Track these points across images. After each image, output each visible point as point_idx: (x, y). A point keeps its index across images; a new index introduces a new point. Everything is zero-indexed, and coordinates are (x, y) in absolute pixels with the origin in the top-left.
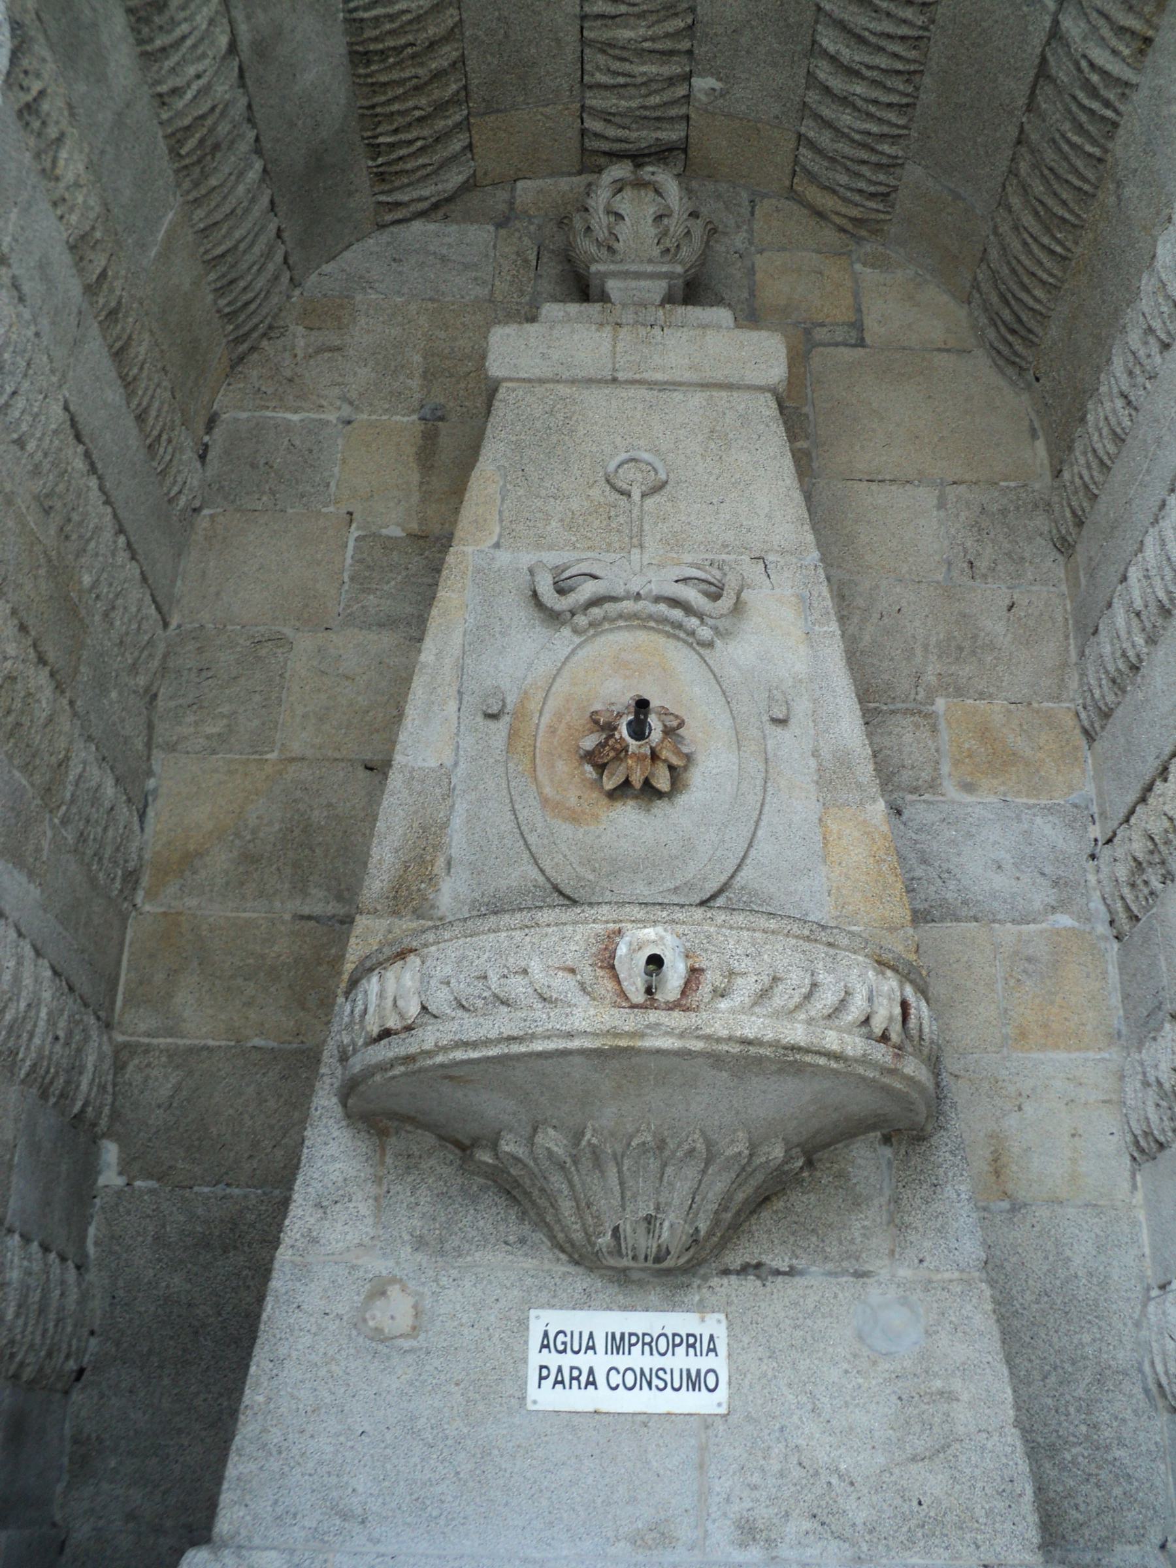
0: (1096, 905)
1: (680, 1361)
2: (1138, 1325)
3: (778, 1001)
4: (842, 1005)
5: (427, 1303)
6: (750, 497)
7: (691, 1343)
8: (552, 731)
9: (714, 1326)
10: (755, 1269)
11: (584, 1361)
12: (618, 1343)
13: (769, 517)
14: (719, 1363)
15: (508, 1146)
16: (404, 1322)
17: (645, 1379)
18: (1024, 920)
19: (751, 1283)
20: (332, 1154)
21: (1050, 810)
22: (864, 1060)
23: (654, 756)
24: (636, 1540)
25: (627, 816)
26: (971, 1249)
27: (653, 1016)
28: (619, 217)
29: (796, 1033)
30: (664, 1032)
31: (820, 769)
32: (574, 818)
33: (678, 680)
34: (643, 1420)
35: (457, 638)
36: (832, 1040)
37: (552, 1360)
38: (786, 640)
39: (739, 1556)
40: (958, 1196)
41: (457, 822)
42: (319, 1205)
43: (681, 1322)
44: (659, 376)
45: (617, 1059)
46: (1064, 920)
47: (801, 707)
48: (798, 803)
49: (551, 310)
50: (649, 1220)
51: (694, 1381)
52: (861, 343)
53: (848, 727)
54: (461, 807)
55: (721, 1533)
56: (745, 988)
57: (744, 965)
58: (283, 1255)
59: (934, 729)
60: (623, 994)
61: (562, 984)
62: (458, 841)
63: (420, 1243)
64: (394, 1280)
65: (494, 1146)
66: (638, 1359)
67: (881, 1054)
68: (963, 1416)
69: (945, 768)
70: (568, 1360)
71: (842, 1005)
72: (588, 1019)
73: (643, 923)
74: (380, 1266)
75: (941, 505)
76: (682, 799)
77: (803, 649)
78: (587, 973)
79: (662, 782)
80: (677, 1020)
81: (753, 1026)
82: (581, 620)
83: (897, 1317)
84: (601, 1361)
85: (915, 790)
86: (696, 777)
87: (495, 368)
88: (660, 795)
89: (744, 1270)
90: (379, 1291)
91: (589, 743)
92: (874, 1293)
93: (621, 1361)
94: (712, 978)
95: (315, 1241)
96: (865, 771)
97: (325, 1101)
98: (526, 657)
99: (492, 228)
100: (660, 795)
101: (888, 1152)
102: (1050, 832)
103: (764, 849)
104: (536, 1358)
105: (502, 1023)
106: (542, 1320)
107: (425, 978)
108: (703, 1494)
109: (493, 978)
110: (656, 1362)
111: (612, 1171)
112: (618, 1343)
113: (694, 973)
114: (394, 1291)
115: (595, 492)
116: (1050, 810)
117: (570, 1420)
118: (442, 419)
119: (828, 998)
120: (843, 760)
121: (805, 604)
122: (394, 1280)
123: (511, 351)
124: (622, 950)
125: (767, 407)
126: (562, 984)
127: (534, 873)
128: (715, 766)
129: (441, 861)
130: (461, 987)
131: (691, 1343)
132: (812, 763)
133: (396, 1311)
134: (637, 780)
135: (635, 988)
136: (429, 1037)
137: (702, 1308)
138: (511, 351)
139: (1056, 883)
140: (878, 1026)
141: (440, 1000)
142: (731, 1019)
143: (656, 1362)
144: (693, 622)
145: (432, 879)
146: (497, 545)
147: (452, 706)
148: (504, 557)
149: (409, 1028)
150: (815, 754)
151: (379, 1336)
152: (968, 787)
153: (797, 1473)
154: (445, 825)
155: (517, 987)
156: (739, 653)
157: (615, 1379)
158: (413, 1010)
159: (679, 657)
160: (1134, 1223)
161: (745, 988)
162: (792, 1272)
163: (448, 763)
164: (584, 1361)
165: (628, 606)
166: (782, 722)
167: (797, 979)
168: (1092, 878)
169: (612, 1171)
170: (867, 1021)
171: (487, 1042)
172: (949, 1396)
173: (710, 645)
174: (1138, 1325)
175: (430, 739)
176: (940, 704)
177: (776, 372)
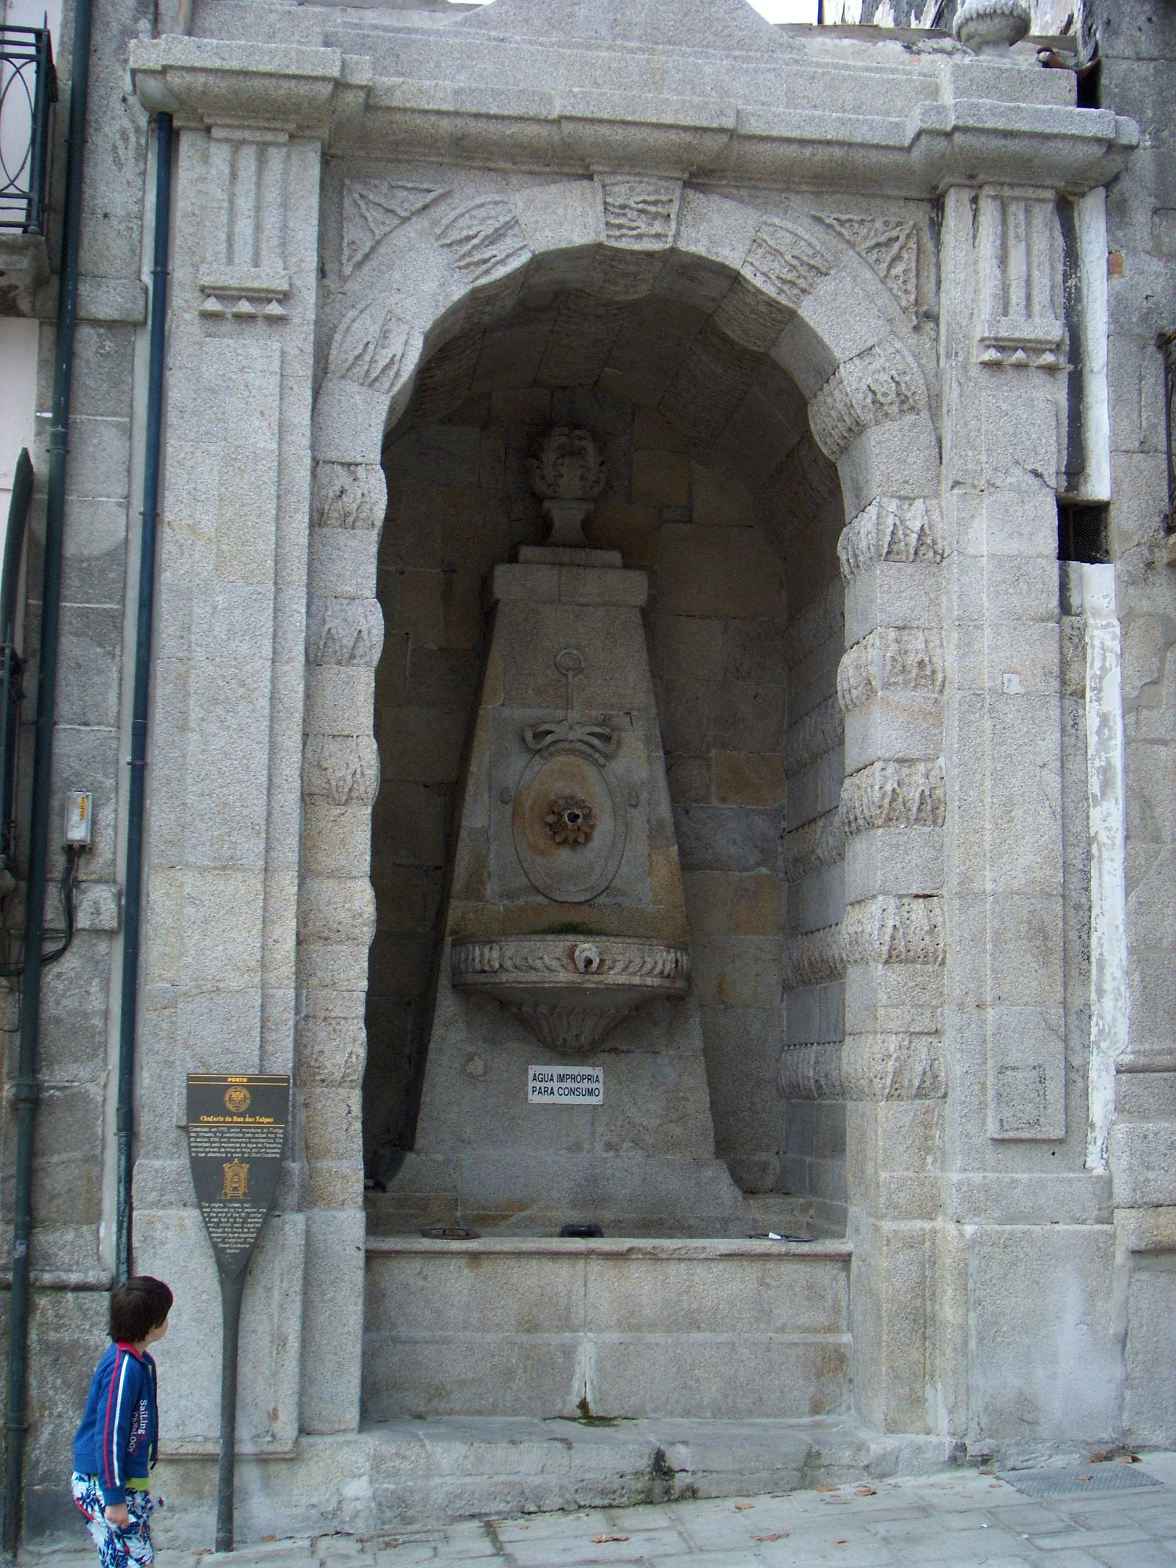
0: (780, 863)
1: (585, 1085)
2: (777, 1061)
3: (631, 970)
4: (653, 968)
5: (489, 1063)
6: (625, 680)
7: (590, 1078)
8: (532, 808)
9: (598, 1072)
10: (615, 1050)
11: (549, 1085)
12: (562, 1078)
13: (634, 688)
14: (600, 1086)
15: (525, 1009)
16: (481, 1070)
17: (572, 1092)
18: (745, 869)
19: (613, 1056)
20: (447, 1005)
21: (763, 813)
22: (660, 986)
23: (579, 829)
24: (569, 1149)
25: (565, 854)
26: (698, 1043)
27: (587, 977)
28: (561, 476)
29: (637, 980)
30: (592, 982)
31: (651, 829)
32: (543, 854)
33: (591, 787)
34: (572, 1107)
35: (486, 758)
36: (649, 981)
37: (538, 1084)
38: (638, 760)
39: (605, 1155)
40: (695, 1023)
41: (492, 856)
42: (444, 1025)
43: (586, 1070)
44: (582, 600)
45: (574, 990)
46: (764, 870)
47: (644, 796)
48: (640, 847)
49: (526, 552)
50: (577, 1036)
51: (590, 1092)
52: (690, 521)
53: (664, 809)
54: (493, 848)
55: (599, 1147)
56: (619, 966)
57: (619, 957)
58: (432, 1045)
59: (709, 768)
60: (577, 968)
61: (554, 964)
62: (493, 866)
63: (485, 1040)
64: (475, 1054)
65: (520, 1006)
66: (570, 1084)
67: (667, 983)
68: (690, 1107)
69: (713, 789)
70: (543, 1084)
71: (653, 968)
72: (564, 977)
73: (585, 942)
74: (471, 1049)
75: (725, 633)
76: (590, 845)
77: (646, 765)
78: (565, 961)
79: (582, 840)
80: (596, 978)
81: (622, 979)
82: (545, 754)
83: (668, 1069)
84: (555, 1085)
85: (697, 801)
86: (596, 834)
87: (500, 591)
88: (579, 843)
89: (610, 1051)
90: (470, 1058)
91: (550, 819)
92: (659, 1060)
93: (563, 1085)
94: (608, 963)
95: (444, 1039)
96: (670, 830)
97: (444, 982)
98: (518, 770)
99: (478, 429)
100: (579, 843)
101: (668, 1004)
102: (762, 824)
103: (624, 869)
104: (531, 1084)
105: (532, 977)
106: (534, 1070)
107: (502, 957)
108: (593, 1134)
109: (530, 961)
110: (576, 1085)
111: (565, 1018)
112: (562, 1078)
113: (602, 961)
114: (476, 1058)
115: (549, 672)
116: (763, 813)
117: (544, 1107)
118: (453, 571)
119: (649, 966)
120: (661, 824)
121: (648, 740)
122: (475, 1054)
123: (509, 582)
124: (577, 953)
125: (636, 618)
126: (554, 964)
128: (604, 827)
129: (485, 875)
130: (518, 961)
131: (590, 1078)
132: (647, 826)
133: (477, 1066)
134: (571, 839)
135: (581, 966)
136: (504, 977)
137: (594, 1065)
138: (509, 582)
139: (762, 851)
140: (666, 971)
141: (508, 964)
142: (615, 977)
143: (576, 1085)
144: (597, 755)
145: (482, 883)
146: (503, 705)
147: (486, 795)
148: (506, 712)
149: (495, 972)
150: (649, 821)
151: (471, 1076)
152: (723, 800)
153: (628, 1126)
154: (487, 855)
155: (538, 964)
156: (618, 767)
157: (561, 1092)
158: (497, 966)
159: (590, 771)
160: (781, 1016)
161: (619, 966)
162: (628, 1051)
163: (486, 825)
164: (549, 1085)
165: (566, 745)
166: (635, 806)
167: (638, 961)
168: (780, 849)
169: (565, 1018)
170: (662, 972)
171: (527, 982)
172: (686, 1099)
173: (604, 766)
174: (777, 1061)
175: (477, 814)
176: (713, 752)
177: (642, 598)
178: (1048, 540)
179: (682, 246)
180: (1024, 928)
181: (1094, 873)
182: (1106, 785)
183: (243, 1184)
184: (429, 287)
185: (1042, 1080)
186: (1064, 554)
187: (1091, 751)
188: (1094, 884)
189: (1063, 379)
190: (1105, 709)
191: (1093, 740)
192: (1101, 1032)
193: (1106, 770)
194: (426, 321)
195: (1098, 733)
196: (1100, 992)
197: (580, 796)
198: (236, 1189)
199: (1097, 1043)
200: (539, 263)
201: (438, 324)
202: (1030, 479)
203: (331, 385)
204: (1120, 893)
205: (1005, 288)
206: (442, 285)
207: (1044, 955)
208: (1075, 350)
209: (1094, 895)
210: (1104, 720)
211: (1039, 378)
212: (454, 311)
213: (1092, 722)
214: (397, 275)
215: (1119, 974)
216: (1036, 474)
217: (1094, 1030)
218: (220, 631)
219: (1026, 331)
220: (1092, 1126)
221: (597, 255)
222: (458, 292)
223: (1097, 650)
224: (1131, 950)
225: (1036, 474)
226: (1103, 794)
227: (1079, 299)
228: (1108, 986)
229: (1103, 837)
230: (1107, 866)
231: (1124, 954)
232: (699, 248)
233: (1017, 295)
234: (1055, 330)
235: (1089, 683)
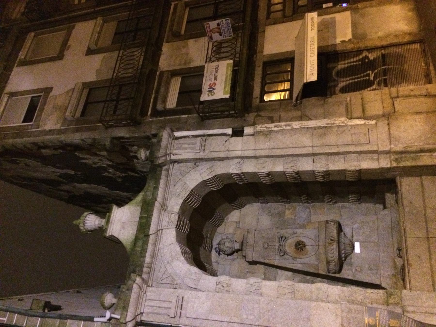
52: (239, 222)
127: (314, 256)
178: (239, 139)
179: (177, 211)
180: (320, 139)
181: (307, 127)
182: (289, 125)
183: (395, 321)
184: (181, 264)
185: (355, 134)
186: (243, 136)
187: (282, 129)
188: (310, 126)
189: (208, 138)
190: (273, 126)
191: (279, 128)
192: (343, 123)
193: (286, 126)
194: (188, 266)
195: (278, 127)
196: (334, 124)
197: (295, 244)
198: (397, 323)
199: (345, 124)
200: (179, 240)
201: (189, 262)
202: (226, 142)
203: (199, 288)
204: (312, 121)
205: (190, 148)
206: (180, 261)
207: (325, 135)
208: (204, 136)
209: (313, 126)
210: (275, 126)
211: (207, 142)
212: (186, 259)
213: (276, 129)
214: (177, 272)
215: (330, 120)
216: (226, 141)
217: (343, 124)
218: (252, 317)
219: (198, 144)
220: (365, 123)
221: (178, 228)
222: (182, 258)
223: (262, 129)
224: (324, 118)
225: (226, 141)
226: (290, 126)
227: (194, 136)
228: (332, 122)
229: (300, 125)
230: (306, 124)
231: (325, 120)
232: (178, 207)
233: (191, 146)
234: (199, 139)
235: (268, 130)
